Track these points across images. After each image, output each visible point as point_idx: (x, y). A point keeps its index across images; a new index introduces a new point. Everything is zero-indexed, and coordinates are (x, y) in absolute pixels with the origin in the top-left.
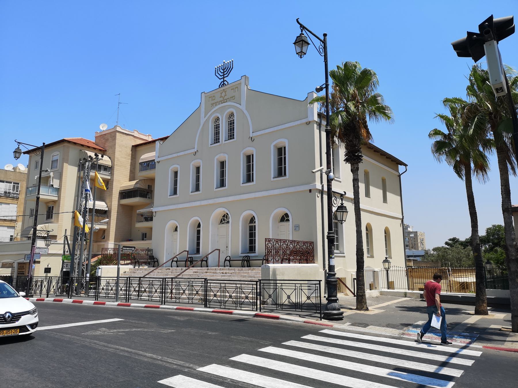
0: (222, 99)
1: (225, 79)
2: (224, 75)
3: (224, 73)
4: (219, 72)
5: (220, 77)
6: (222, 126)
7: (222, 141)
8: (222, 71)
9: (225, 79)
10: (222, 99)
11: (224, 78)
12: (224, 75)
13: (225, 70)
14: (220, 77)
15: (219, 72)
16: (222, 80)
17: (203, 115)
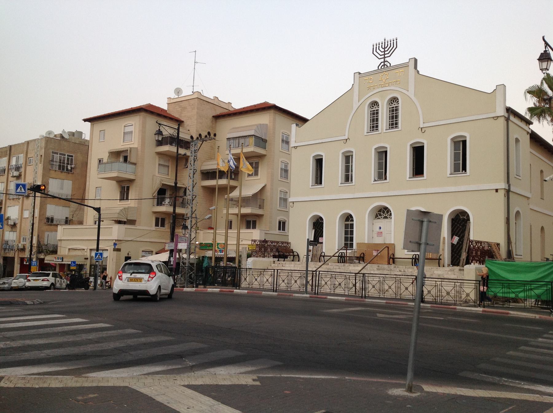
1: (387, 59)
2: (385, 54)
3: (385, 51)
4: (378, 51)
5: (380, 57)
6: (382, 113)
7: (382, 129)
8: (383, 50)
9: (387, 59)
11: (385, 57)
12: (385, 54)
13: (386, 49)
14: (380, 57)
15: (378, 51)
16: (383, 60)
17: (356, 98)
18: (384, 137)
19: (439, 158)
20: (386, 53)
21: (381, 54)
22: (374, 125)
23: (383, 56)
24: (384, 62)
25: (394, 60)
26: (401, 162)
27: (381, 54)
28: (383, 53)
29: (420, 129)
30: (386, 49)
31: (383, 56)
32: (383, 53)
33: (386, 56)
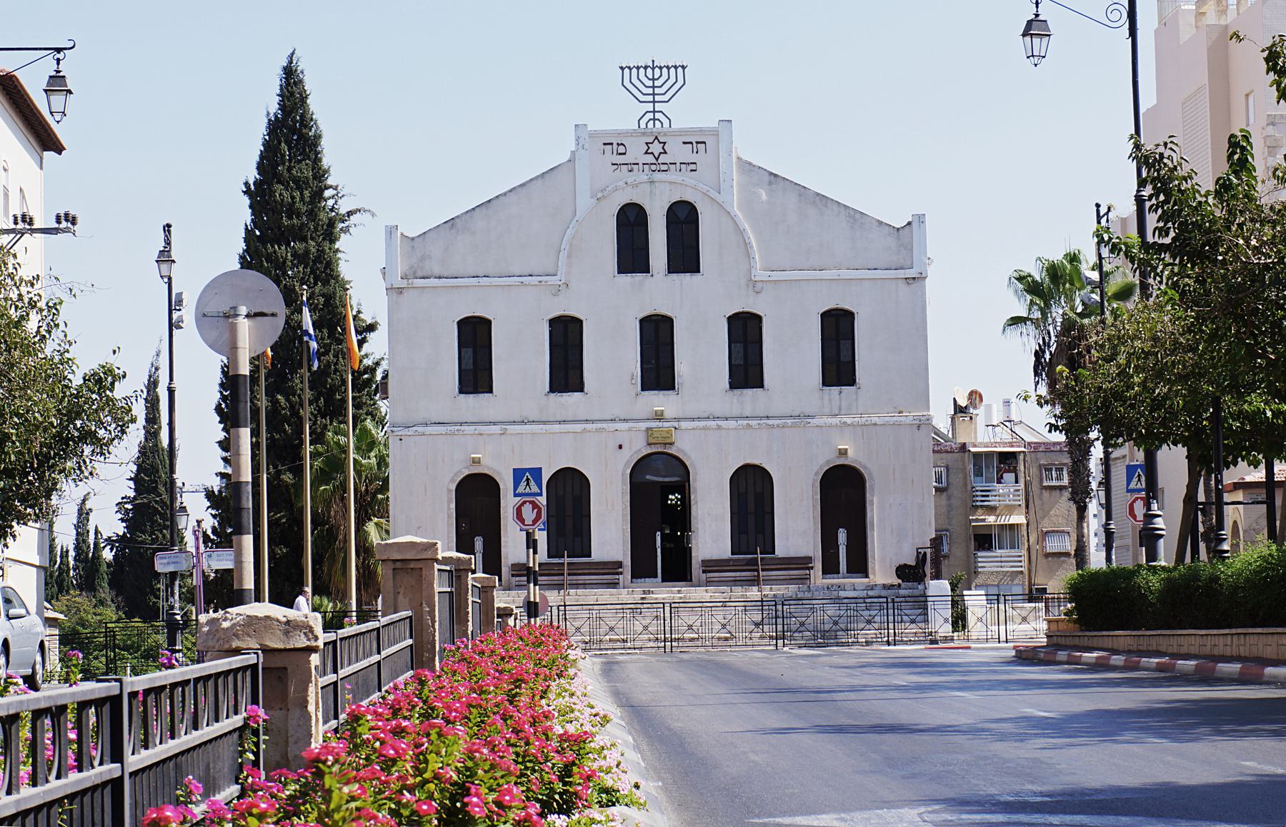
0: (650, 159)
1: (658, 107)
8: (650, 83)
9: (658, 107)
10: (650, 159)
11: (654, 102)
13: (654, 80)
16: (650, 107)
18: (659, 290)
19: (792, 353)
20: (657, 91)
21: (645, 91)
22: (632, 257)
23: (650, 98)
24: (654, 112)
25: (683, 114)
26: (702, 354)
27: (645, 91)
28: (650, 91)
29: (751, 285)
30: (657, 83)
31: (650, 98)
32: (650, 91)
33: (657, 98)
